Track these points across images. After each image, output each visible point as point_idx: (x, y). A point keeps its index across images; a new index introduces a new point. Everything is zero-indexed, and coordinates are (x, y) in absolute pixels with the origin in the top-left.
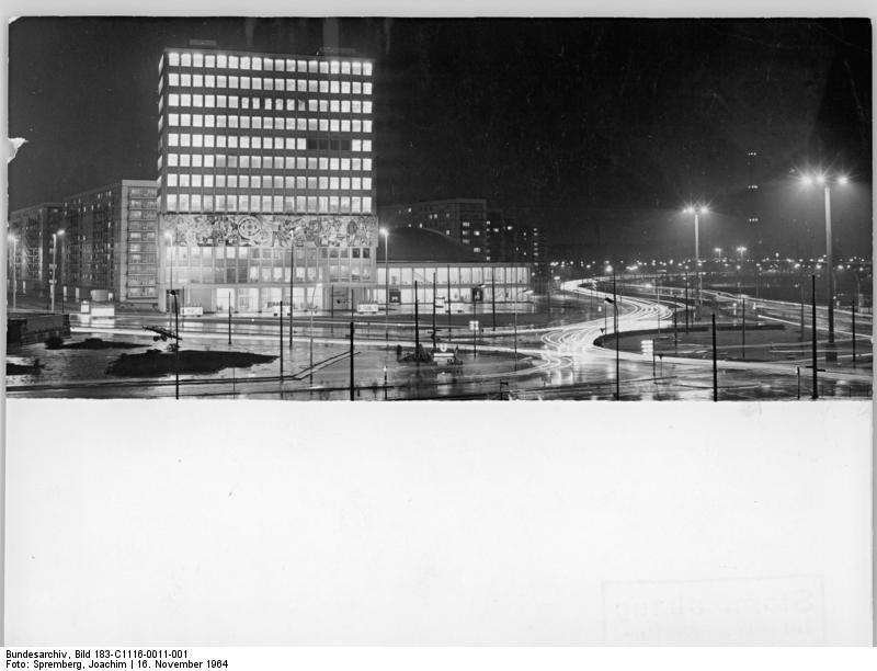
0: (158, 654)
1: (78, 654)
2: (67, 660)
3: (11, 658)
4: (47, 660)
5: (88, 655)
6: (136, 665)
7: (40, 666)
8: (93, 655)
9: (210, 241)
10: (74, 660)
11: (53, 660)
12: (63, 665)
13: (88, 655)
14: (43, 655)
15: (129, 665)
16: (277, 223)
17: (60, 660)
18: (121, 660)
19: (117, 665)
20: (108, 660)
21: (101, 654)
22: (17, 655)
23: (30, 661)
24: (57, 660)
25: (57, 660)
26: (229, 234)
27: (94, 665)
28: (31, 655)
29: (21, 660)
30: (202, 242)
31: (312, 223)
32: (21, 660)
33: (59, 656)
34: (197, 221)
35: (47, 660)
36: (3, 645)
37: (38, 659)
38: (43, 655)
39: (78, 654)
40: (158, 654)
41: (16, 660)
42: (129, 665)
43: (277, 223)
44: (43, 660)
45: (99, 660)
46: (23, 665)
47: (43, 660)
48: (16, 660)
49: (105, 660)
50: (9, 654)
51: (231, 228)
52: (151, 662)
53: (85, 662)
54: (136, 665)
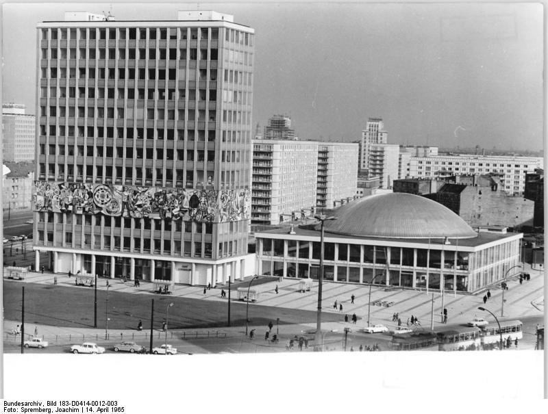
2: (42, 407)
3: (7, 406)
4: (30, 407)
5: (55, 404)
6: (85, 410)
7: (25, 411)
8: (58, 404)
9: (70, 208)
10: (46, 407)
11: (33, 407)
12: (39, 410)
13: (55, 404)
14: (27, 404)
15: (81, 410)
16: (126, 193)
17: (38, 407)
18: (75, 407)
19: (73, 410)
20: (68, 407)
21: (63, 403)
23: (19, 408)
24: (35, 407)
25: (35, 407)
26: (85, 202)
27: (59, 410)
28: (19, 404)
29: (13, 407)
30: (64, 208)
31: (157, 195)
32: (13, 407)
34: (61, 188)
35: (30, 407)
36: (3, 398)
37: (24, 406)
38: (27, 404)
39: (49, 403)
41: (10, 407)
42: (81, 410)
45: (62, 407)
48: (10, 407)
49: (65, 407)
50: (5, 403)
51: (87, 196)
52: (95, 408)
53: (53, 408)
54: (85, 410)
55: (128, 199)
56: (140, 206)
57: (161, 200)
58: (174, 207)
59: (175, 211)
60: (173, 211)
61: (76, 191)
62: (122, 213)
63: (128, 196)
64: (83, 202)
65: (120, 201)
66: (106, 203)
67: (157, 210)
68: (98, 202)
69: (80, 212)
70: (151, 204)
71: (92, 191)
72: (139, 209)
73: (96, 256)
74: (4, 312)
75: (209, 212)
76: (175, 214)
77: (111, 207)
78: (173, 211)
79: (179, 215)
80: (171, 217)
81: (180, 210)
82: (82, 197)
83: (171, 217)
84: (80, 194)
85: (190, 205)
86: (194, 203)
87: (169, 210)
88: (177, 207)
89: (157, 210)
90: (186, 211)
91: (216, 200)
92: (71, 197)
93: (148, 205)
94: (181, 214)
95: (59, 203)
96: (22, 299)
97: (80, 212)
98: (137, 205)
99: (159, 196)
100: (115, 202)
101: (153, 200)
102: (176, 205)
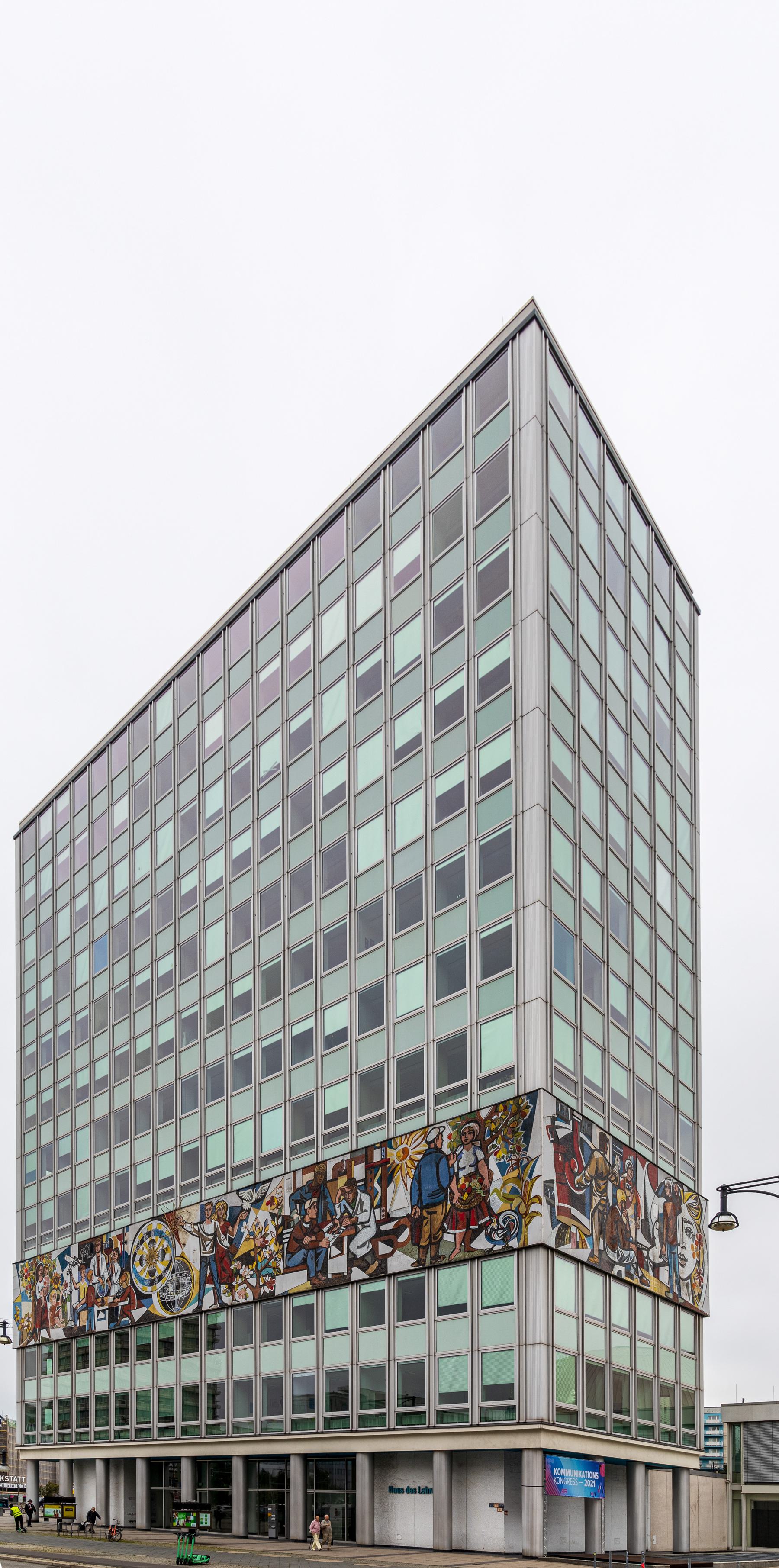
9: (83, 1321)
16: (209, 1228)
26: (115, 1290)
34: (64, 1264)
43: (209, 1228)
51: (117, 1267)
55: (215, 1244)
56: (247, 1259)
57: (312, 1213)
58: (354, 1228)
59: (360, 1245)
60: (353, 1247)
61: (94, 1260)
62: (200, 1299)
63: (215, 1234)
64: (108, 1294)
65: (196, 1266)
66: (160, 1278)
67: (299, 1256)
68: (142, 1281)
69: (102, 1325)
70: (279, 1239)
71: (128, 1248)
72: (246, 1271)
73: (306, 1458)
75: (497, 1203)
76: (360, 1253)
77: (172, 1288)
78: (353, 1247)
79: (374, 1251)
80: (343, 1270)
81: (379, 1235)
82: (106, 1276)
83: (343, 1270)
84: (104, 1267)
85: (418, 1201)
86: (429, 1186)
87: (339, 1244)
88: (365, 1224)
89: (299, 1256)
90: (397, 1231)
91: (527, 1138)
92: (84, 1285)
93: (273, 1247)
94: (383, 1249)
95: (60, 1314)
97: (102, 1325)
98: (238, 1259)
99: (302, 1202)
100: (184, 1266)
101: (287, 1221)
102: (363, 1217)
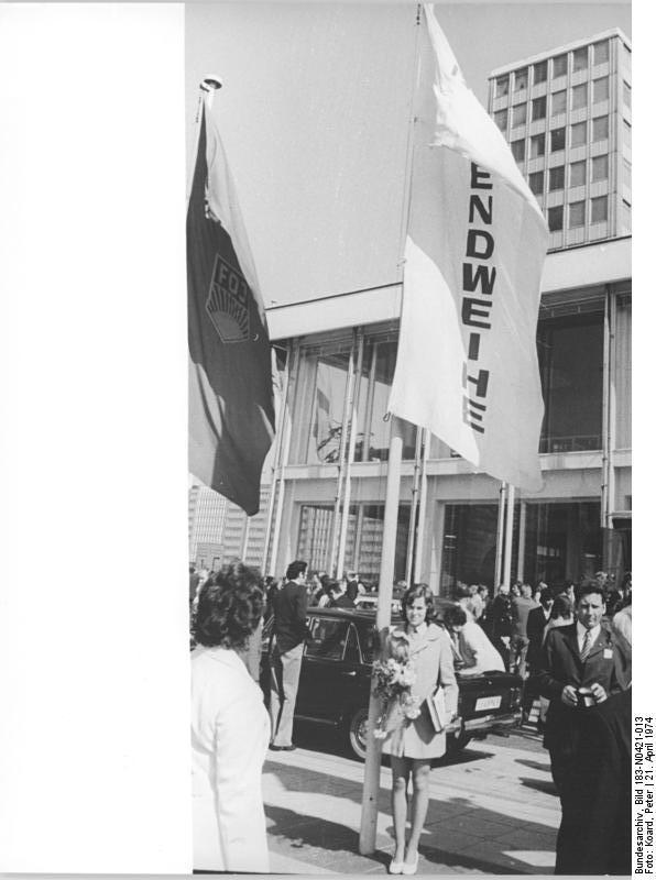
0: (639, 727)
1: (639, 802)
3: (643, 869)
5: (640, 792)
8: (640, 787)
14: (640, 837)
22: (640, 863)
23: (646, 850)
28: (640, 849)
29: (645, 859)
32: (645, 859)
33: (641, 821)
38: (640, 837)
40: (639, 727)
41: (645, 864)
44: (645, 836)
46: (652, 857)
47: (645, 837)
48: (645, 864)
50: (639, 871)
74: (610, 874)
96: (230, 869)
